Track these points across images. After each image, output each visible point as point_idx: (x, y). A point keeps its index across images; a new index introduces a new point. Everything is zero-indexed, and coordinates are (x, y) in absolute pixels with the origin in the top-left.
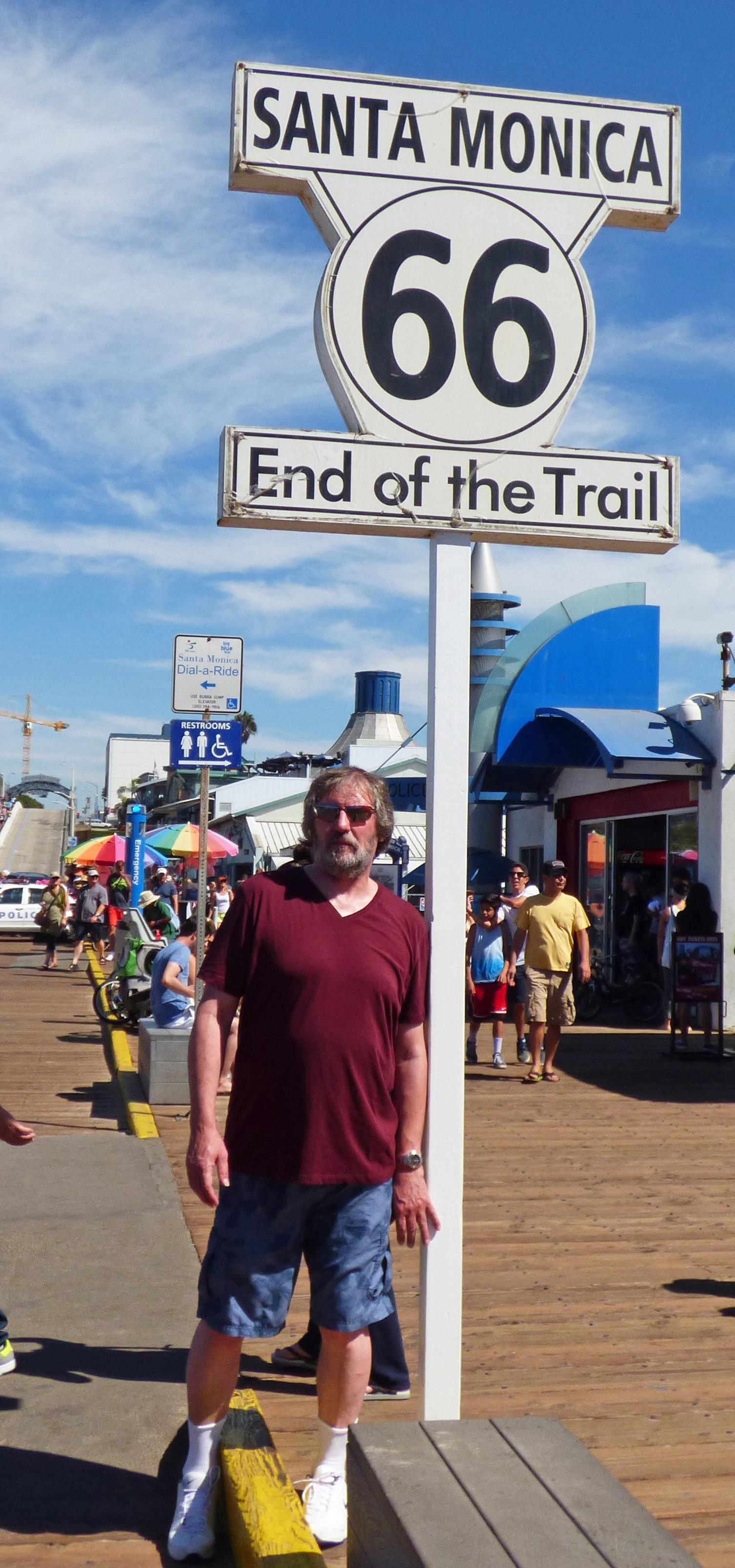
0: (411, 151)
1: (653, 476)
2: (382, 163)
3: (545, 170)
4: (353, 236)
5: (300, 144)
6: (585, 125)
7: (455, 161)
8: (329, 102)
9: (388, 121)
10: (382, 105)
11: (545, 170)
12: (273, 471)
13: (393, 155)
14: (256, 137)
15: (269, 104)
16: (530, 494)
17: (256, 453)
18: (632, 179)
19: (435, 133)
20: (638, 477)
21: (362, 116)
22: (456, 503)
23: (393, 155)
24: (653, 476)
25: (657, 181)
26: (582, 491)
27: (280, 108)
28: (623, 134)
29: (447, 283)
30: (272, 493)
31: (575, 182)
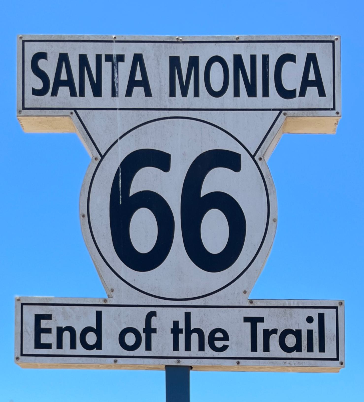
27: (49, 67)
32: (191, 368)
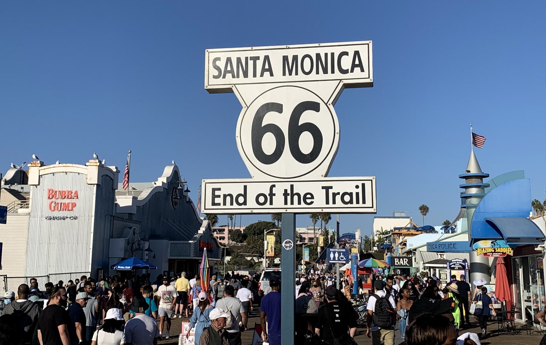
0: (269, 73)
1: (363, 185)
2: (258, 79)
3: (317, 73)
4: (248, 107)
5: (229, 76)
6: (333, 54)
7: (284, 74)
8: (239, 60)
9: (259, 64)
10: (258, 58)
11: (317, 73)
12: (219, 196)
13: (262, 75)
15: (218, 63)
17: (214, 190)
18: (352, 71)
19: (277, 65)
21: (251, 63)
22: (286, 203)
23: (262, 75)
24: (363, 185)
25: (362, 70)
26: (334, 195)
28: (348, 55)
29: (282, 121)
30: (219, 204)
31: (329, 76)
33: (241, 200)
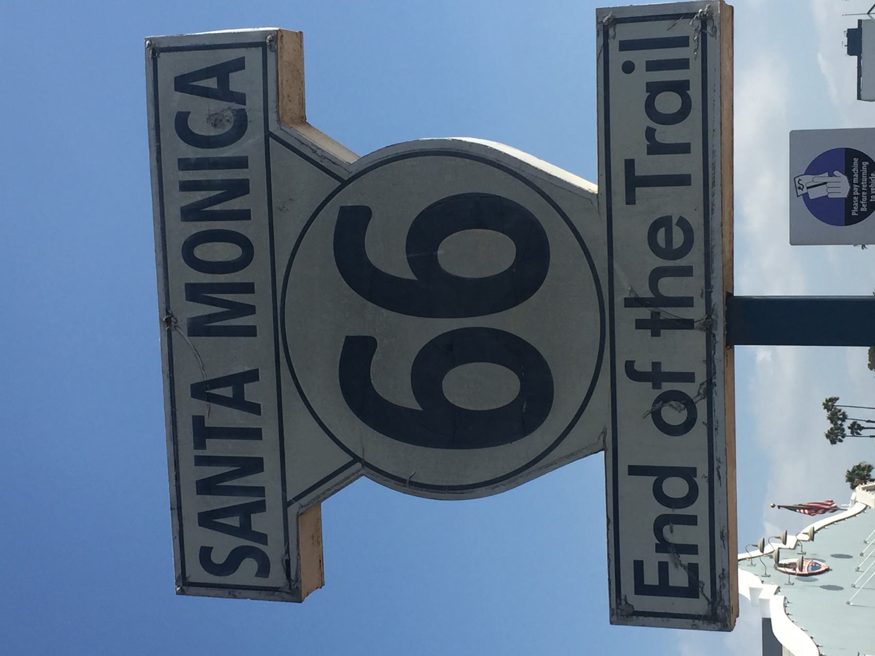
1: (625, 46)
4: (356, 459)
5: (258, 522)
7: (250, 331)
12: (663, 568)
13: (255, 409)
14: (258, 574)
15: (219, 557)
16: (664, 222)
17: (641, 588)
20: (628, 67)
22: (688, 324)
23: (255, 409)
24: (625, 46)
26: (655, 148)
29: (404, 337)
30: (693, 569)
32: (729, 296)
33: (676, 487)
